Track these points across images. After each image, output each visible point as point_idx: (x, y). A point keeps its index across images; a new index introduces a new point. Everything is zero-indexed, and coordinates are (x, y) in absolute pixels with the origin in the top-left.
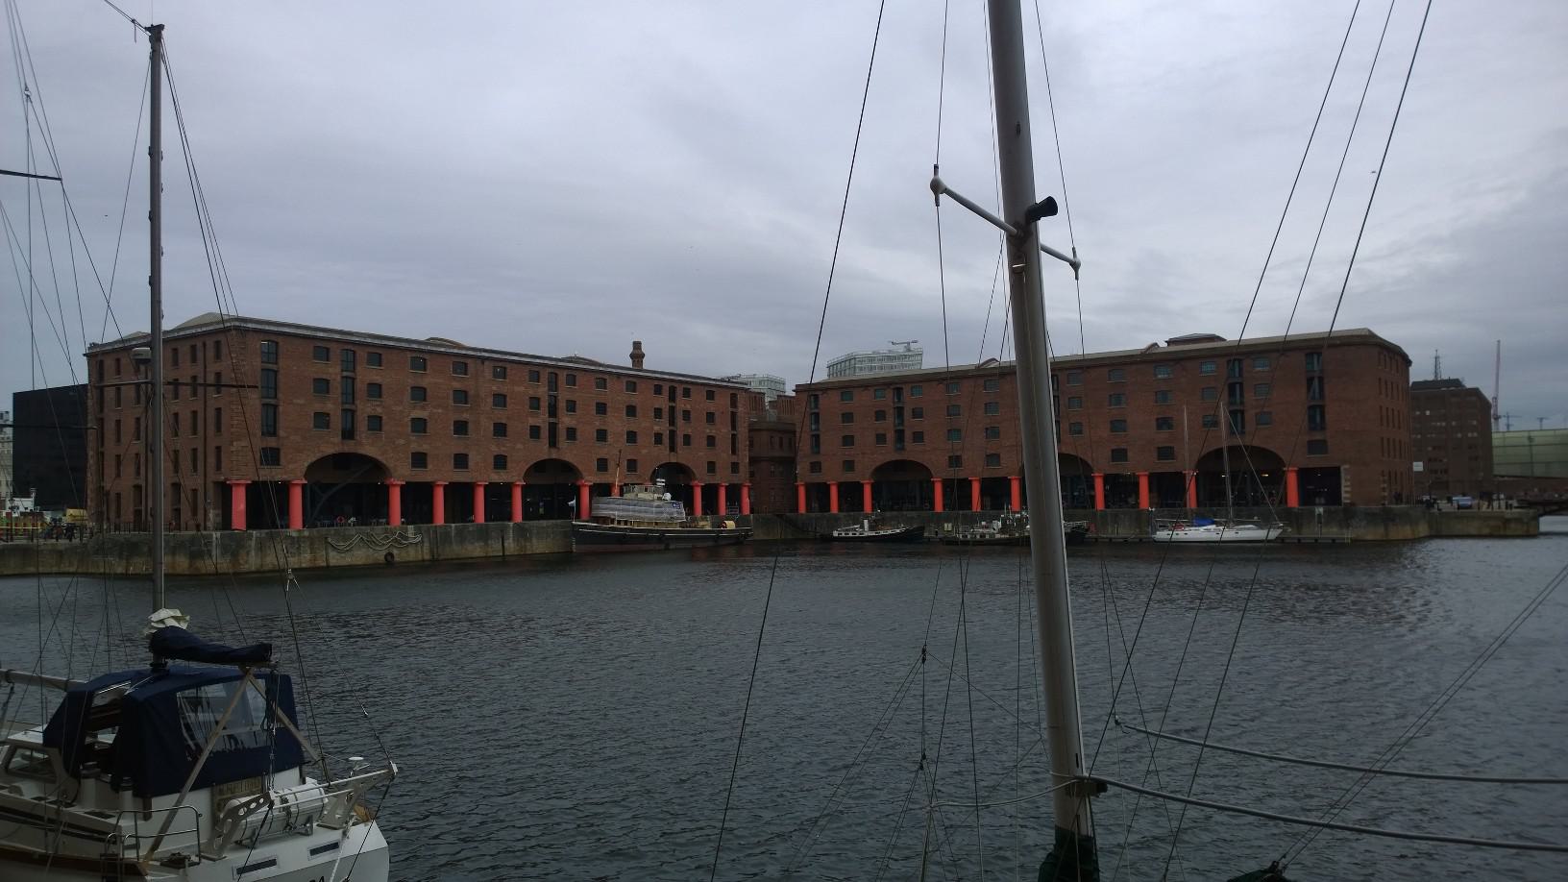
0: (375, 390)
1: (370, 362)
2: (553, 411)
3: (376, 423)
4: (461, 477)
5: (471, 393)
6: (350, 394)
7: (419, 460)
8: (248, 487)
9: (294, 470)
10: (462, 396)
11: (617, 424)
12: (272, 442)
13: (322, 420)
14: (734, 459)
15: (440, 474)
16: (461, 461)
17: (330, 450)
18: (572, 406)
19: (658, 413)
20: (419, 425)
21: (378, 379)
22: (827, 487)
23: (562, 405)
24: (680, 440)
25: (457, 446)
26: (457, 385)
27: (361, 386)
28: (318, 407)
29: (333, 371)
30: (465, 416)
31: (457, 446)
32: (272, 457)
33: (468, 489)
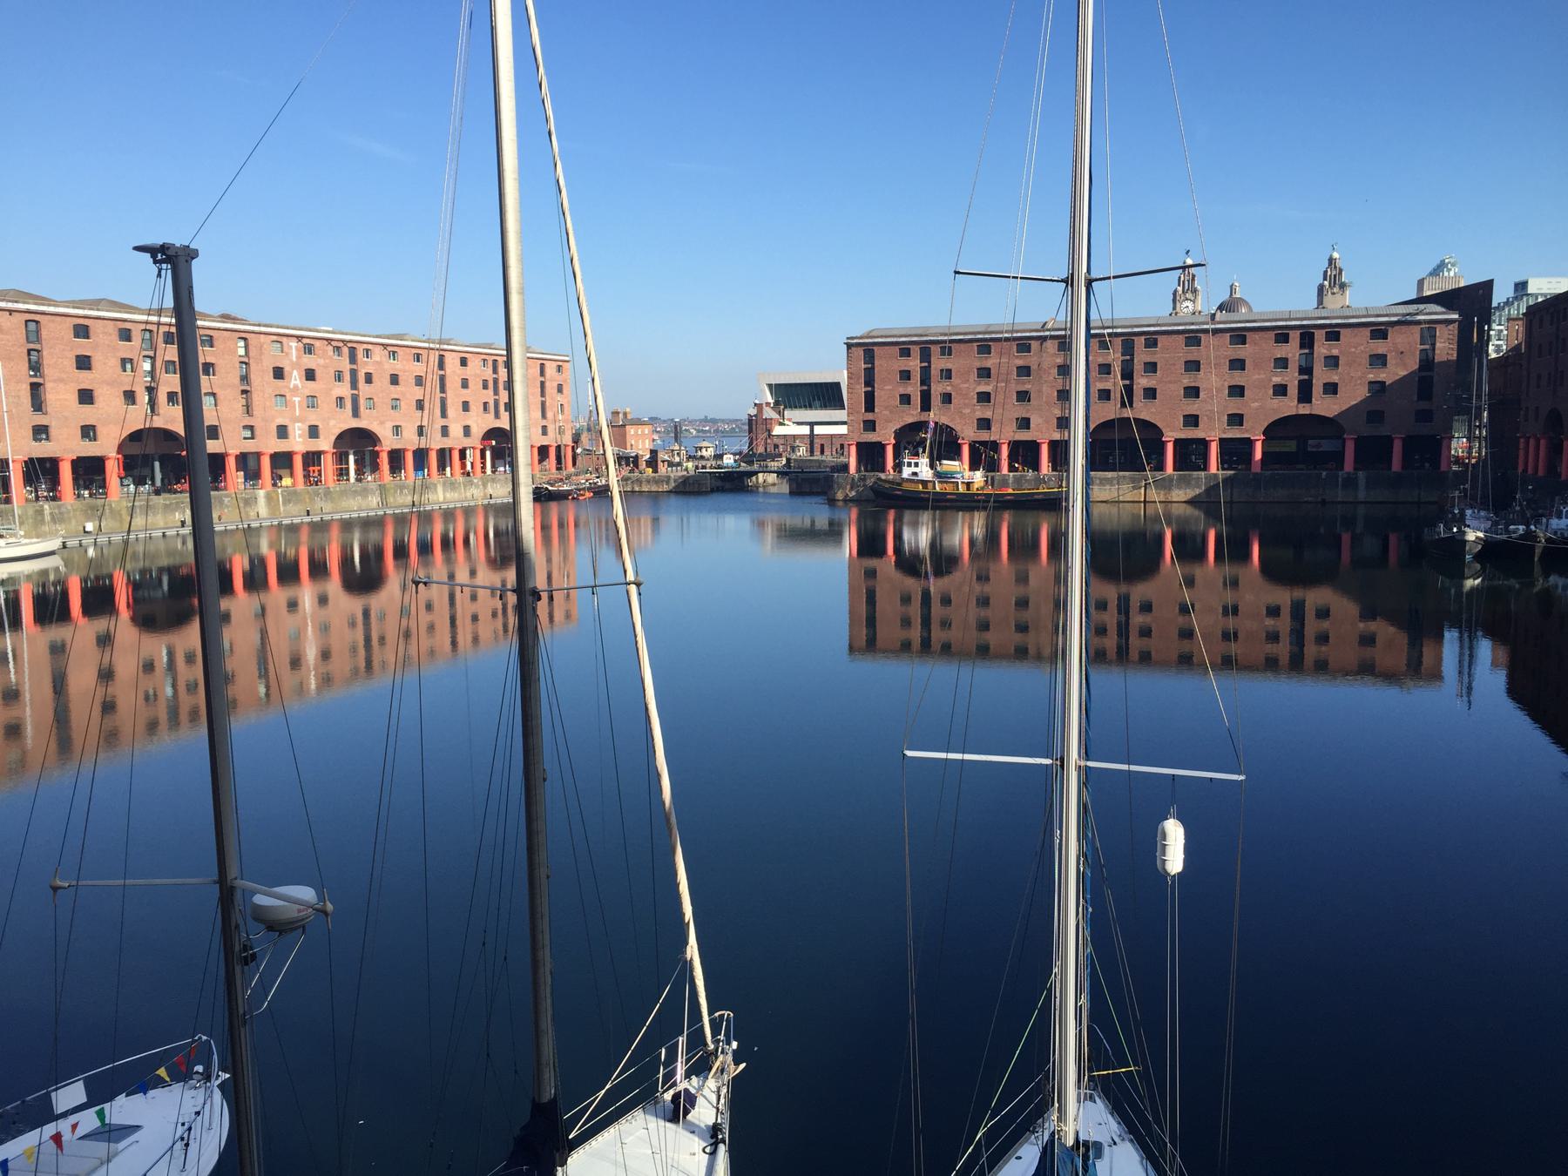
0: (947, 374)
1: (943, 354)
2: (1128, 374)
3: (947, 398)
4: (1024, 436)
5: (1034, 367)
6: (926, 379)
7: (985, 424)
8: (1403, 440)
9: (886, 435)
10: (1024, 371)
11: (1214, 380)
12: (870, 416)
13: (905, 399)
14: (1424, 405)
15: (1005, 434)
16: (1024, 423)
17: (911, 420)
18: (1151, 367)
19: (1282, 363)
20: (984, 398)
21: (949, 366)
22: (1390, 440)
23: (1138, 367)
24: (1317, 389)
25: (1021, 411)
26: (1020, 362)
27: (935, 372)
28: (902, 390)
29: (914, 364)
30: (1027, 387)
31: (1021, 411)
32: (870, 426)
33: (1033, 447)
